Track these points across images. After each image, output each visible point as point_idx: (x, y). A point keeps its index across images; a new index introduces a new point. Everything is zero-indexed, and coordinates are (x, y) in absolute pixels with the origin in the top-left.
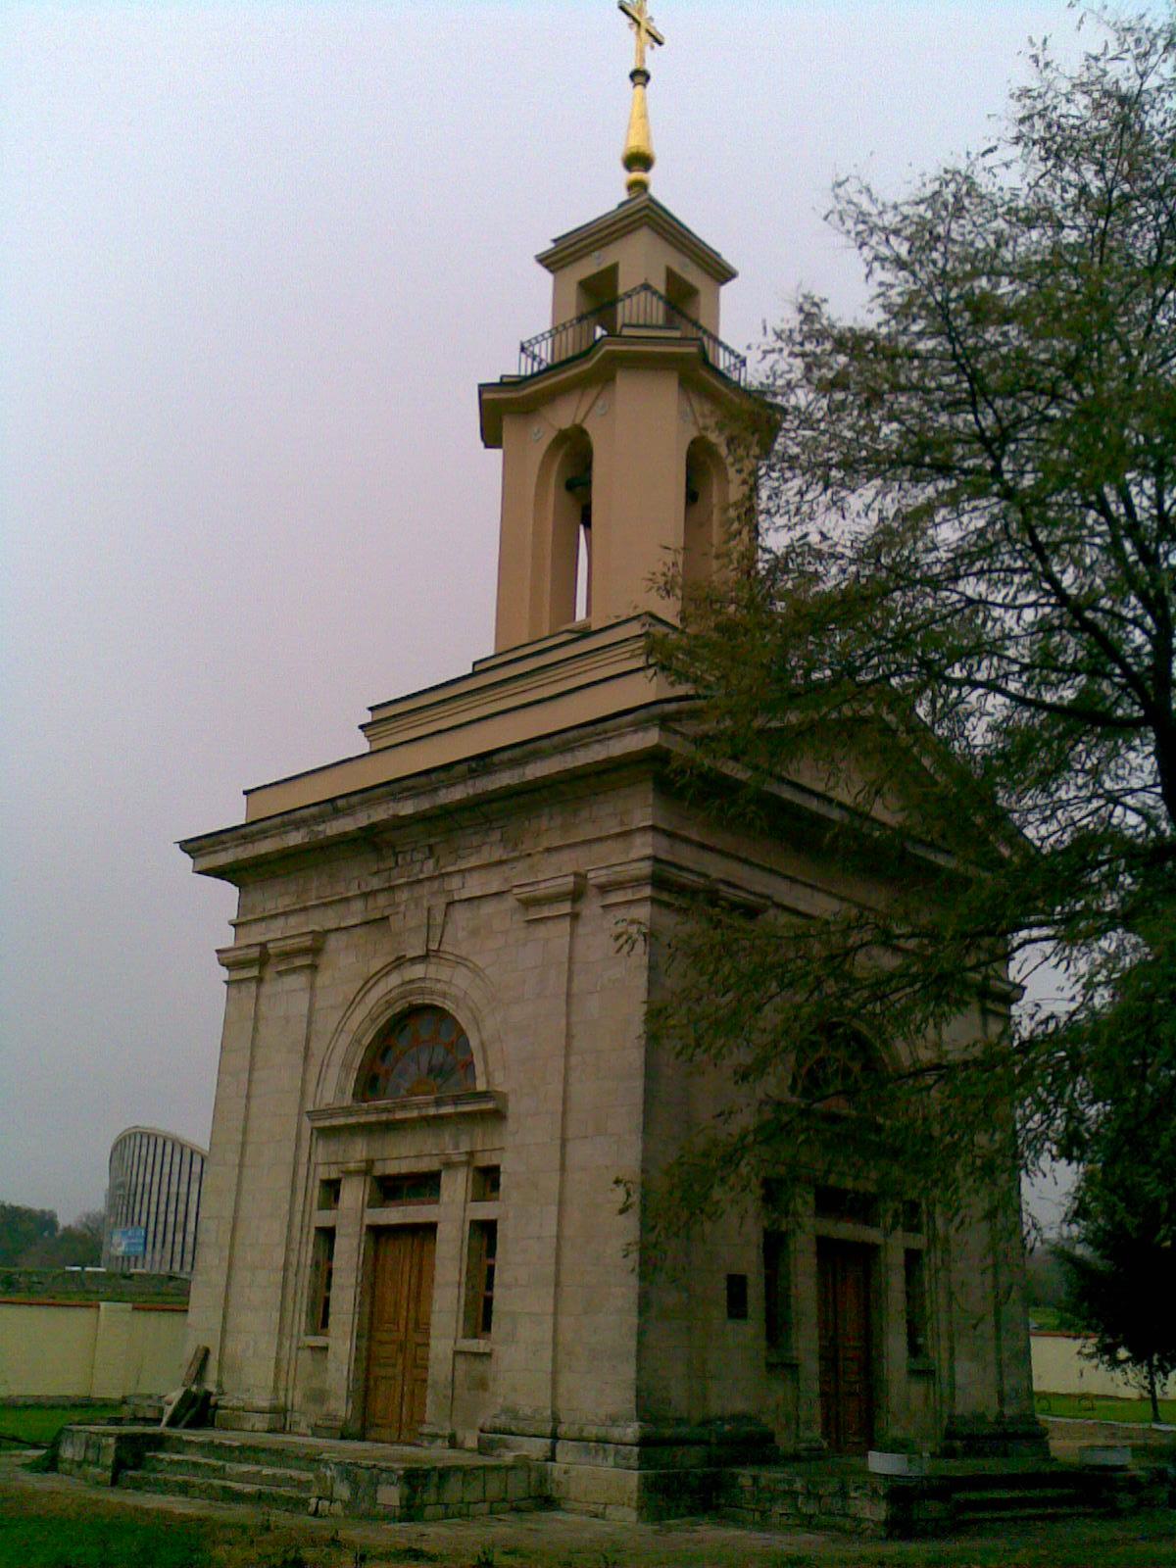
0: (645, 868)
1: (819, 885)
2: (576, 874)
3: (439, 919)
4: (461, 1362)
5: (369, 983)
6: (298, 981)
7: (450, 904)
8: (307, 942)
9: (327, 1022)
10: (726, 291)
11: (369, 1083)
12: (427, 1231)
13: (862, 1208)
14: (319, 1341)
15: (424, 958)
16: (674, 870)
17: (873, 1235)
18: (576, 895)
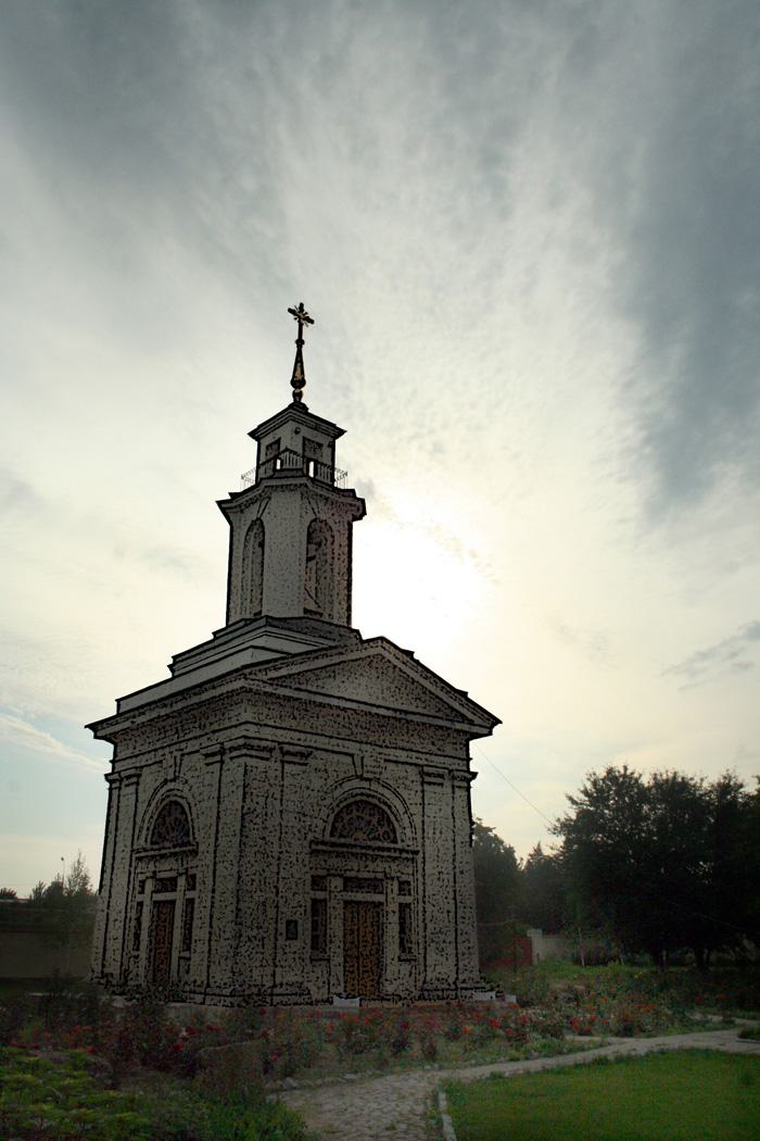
0: (241, 742)
2: (222, 743)
3: (178, 761)
4: (182, 962)
5: (156, 791)
6: (132, 789)
7: (182, 755)
8: (133, 772)
9: (142, 808)
10: (338, 442)
11: (158, 836)
12: (173, 903)
13: (375, 885)
14: (136, 953)
15: (174, 780)
16: (257, 741)
17: (380, 898)
18: (222, 752)
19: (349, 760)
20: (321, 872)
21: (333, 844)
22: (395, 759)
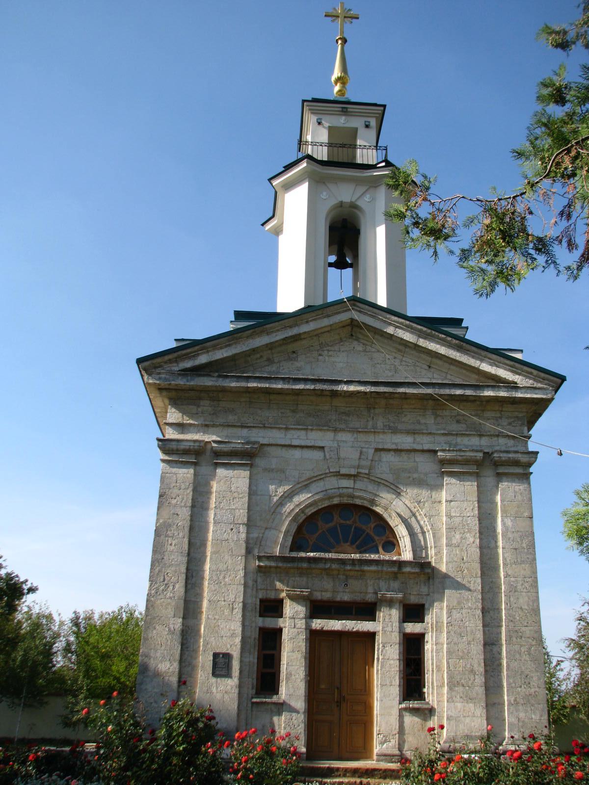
19: (318, 455)
22: (394, 447)
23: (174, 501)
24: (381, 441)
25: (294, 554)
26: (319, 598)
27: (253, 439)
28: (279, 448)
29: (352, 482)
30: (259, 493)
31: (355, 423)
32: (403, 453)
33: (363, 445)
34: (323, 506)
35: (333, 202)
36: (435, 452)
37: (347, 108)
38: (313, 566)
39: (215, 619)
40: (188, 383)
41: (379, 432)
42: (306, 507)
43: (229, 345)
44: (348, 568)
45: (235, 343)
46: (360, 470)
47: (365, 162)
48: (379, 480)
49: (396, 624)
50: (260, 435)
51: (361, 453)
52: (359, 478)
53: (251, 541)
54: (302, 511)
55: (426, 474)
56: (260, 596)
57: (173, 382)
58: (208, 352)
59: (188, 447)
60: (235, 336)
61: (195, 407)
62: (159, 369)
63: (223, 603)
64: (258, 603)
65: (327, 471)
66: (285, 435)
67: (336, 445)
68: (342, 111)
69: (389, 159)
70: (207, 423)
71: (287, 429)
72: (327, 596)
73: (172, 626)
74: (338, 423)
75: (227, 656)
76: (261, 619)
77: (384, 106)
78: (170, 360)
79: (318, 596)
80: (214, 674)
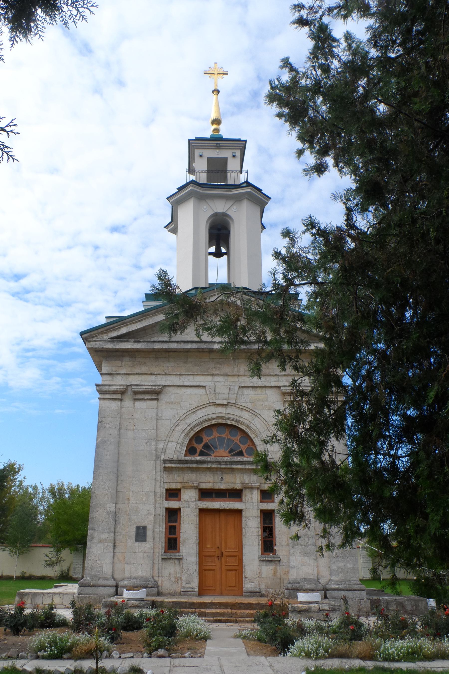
1: (196, 373)
16: (106, 387)
17: (236, 505)
19: (202, 391)
20: (173, 486)
21: (186, 462)
22: (251, 385)
23: (108, 426)
24: (243, 381)
25: (188, 458)
26: (204, 487)
27: (159, 383)
28: (176, 388)
29: (225, 409)
30: (164, 418)
31: (226, 369)
32: (258, 389)
33: (231, 384)
34: (206, 426)
35: (211, 213)
36: (279, 387)
37: (219, 144)
38: (200, 466)
39: (136, 503)
40: (114, 347)
41: (241, 375)
42: (195, 426)
43: (141, 320)
44: (223, 466)
45: (145, 319)
46: (229, 401)
47: (233, 183)
48: (242, 407)
49: (255, 504)
50: (163, 379)
51: (230, 389)
52: (229, 406)
53: (159, 451)
54: (192, 429)
55: (274, 403)
56: (166, 488)
57: (104, 347)
58: (127, 325)
59: (116, 389)
60: (145, 314)
61: (120, 362)
62: (95, 338)
63: (142, 493)
64: (165, 492)
65: (208, 402)
66: (180, 379)
67: (213, 385)
68: (216, 146)
69: (249, 181)
70: (128, 373)
71: (180, 375)
72: (209, 486)
73: (108, 509)
74: (214, 370)
75: (145, 528)
76: (167, 502)
77: (245, 141)
78: (102, 332)
79: (203, 486)
80: (137, 540)
